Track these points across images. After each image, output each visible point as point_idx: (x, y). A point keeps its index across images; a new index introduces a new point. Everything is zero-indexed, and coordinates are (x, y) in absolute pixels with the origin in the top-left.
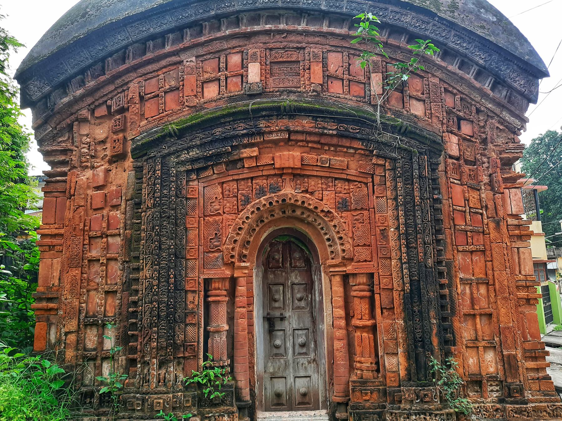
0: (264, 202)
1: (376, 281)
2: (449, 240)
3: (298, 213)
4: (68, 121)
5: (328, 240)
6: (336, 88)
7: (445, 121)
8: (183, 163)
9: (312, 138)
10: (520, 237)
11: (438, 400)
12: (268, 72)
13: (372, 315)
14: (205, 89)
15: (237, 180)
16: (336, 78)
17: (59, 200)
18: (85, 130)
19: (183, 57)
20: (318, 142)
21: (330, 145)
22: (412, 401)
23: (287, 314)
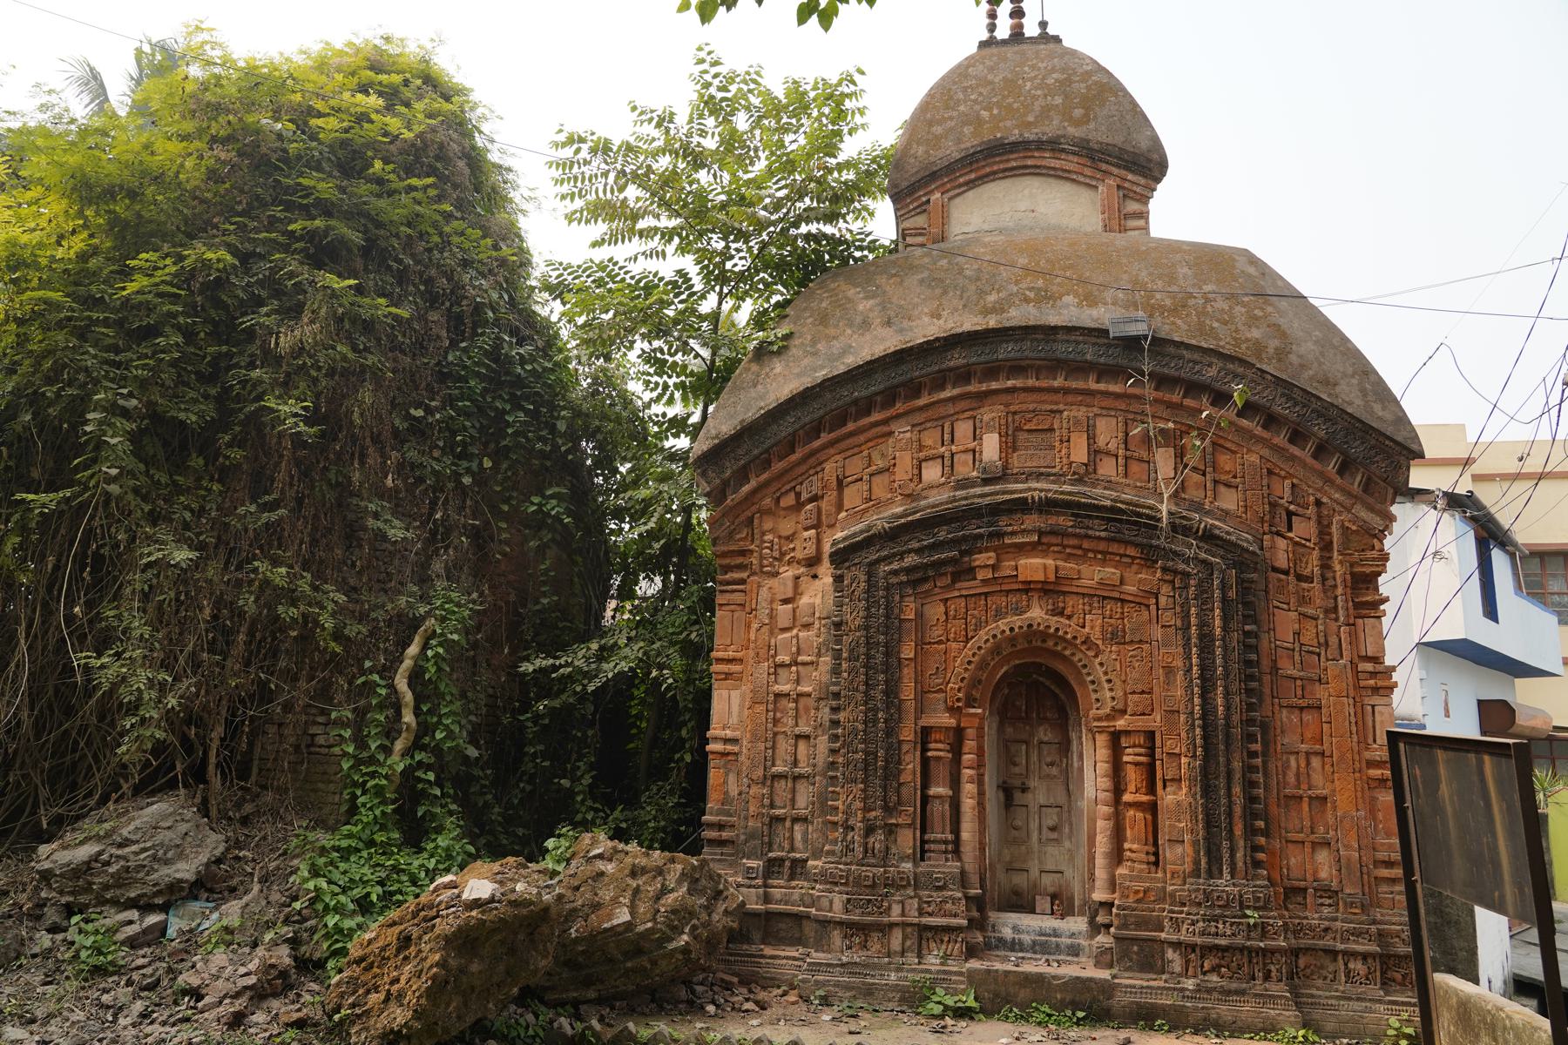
1: (1158, 743)
2: (1267, 691)
3: (1050, 643)
5: (1093, 682)
6: (1107, 468)
7: (1267, 518)
8: (895, 573)
10: (1376, 690)
11: (1236, 904)
13: (1151, 789)
14: (924, 471)
16: (1108, 453)
17: (736, 615)
19: (893, 427)
20: (1080, 547)
22: (1199, 904)
23: (1033, 783)
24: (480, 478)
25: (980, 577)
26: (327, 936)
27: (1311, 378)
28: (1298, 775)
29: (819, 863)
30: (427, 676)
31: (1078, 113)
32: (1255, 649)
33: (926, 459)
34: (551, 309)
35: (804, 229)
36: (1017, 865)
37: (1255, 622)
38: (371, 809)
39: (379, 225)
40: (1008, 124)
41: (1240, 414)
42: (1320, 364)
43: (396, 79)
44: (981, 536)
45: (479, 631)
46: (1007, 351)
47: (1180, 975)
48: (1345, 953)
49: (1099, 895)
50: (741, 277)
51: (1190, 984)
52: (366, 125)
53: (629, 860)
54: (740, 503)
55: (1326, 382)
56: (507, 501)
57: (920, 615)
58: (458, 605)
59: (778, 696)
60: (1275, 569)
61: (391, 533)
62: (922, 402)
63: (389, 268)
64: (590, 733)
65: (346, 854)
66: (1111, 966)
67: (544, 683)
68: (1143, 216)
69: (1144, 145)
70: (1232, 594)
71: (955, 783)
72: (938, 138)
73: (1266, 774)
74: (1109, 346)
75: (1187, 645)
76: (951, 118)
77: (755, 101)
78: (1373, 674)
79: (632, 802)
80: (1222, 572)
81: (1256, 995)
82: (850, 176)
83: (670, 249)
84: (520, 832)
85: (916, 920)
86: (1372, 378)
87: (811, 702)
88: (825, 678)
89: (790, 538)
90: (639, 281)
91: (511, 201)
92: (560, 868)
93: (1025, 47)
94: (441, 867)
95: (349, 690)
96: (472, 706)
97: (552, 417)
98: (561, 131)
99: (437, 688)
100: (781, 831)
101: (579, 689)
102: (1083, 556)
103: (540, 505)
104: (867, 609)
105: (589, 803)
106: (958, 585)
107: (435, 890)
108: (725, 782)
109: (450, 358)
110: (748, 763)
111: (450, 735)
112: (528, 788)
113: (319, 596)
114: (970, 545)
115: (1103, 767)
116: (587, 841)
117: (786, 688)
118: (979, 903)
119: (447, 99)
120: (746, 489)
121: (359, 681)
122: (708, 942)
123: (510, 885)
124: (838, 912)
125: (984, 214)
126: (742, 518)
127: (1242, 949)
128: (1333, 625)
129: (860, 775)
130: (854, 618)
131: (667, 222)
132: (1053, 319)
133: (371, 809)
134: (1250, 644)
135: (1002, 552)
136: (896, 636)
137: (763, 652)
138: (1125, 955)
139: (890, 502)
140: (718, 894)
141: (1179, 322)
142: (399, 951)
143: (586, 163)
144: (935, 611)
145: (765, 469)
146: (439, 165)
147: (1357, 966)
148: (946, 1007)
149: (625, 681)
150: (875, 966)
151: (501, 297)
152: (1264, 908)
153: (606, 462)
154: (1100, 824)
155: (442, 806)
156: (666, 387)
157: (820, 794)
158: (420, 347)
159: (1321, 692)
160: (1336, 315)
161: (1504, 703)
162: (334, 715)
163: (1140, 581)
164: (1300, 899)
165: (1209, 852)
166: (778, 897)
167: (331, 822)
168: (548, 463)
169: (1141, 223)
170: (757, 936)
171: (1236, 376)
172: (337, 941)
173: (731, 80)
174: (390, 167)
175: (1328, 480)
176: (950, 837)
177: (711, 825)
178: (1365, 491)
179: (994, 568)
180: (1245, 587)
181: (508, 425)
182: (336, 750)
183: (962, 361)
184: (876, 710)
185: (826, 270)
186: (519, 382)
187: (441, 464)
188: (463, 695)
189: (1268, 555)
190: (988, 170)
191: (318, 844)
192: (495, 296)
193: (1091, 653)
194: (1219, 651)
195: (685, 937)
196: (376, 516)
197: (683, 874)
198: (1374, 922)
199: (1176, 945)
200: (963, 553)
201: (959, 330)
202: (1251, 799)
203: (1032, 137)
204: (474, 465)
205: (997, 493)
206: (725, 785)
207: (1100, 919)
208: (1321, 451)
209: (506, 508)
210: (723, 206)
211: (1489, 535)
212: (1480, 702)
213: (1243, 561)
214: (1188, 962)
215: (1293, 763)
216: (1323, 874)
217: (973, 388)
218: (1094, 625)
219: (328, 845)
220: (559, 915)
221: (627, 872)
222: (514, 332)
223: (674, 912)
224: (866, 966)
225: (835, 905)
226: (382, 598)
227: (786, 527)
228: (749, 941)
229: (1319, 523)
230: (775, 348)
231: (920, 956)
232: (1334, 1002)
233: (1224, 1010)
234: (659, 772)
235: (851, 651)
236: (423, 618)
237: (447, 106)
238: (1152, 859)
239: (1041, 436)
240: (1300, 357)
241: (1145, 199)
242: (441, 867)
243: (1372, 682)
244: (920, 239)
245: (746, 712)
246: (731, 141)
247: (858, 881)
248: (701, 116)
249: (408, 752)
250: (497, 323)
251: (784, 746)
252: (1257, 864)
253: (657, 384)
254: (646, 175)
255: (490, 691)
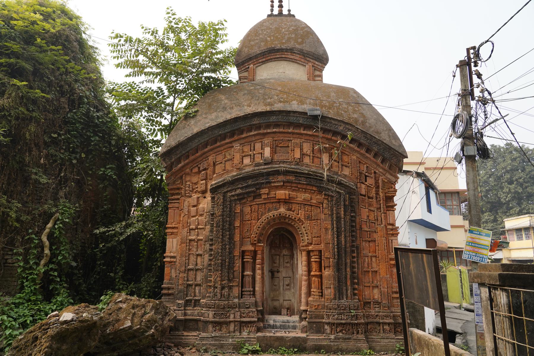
0: (271, 215)
1: (323, 254)
2: (358, 236)
3: (287, 220)
4: (181, 174)
6: (307, 160)
8: (233, 196)
9: (295, 185)
10: (393, 235)
12: (274, 152)
13: (320, 270)
15: (258, 204)
16: (307, 155)
17: (176, 211)
18: (188, 179)
19: (234, 144)
20: (297, 187)
21: (302, 189)
22: (336, 309)
24: (81, 161)
25: (263, 197)
26: (6, 338)
27: (373, 131)
28: (368, 264)
29: (204, 301)
30: (55, 235)
31: (300, 40)
32: (354, 221)
33: (245, 156)
34: (109, 100)
35: (206, 74)
36: (275, 298)
37: (354, 213)
38: (30, 287)
39: (41, 64)
40: (276, 42)
41: (350, 143)
42: (376, 126)
43: (49, 10)
44: (263, 183)
45: (79, 218)
46: (273, 119)
47: (329, 334)
48: (383, 323)
49: (303, 308)
50: (182, 91)
51: (332, 337)
52: (36, 26)
53: (132, 302)
54: (178, 171)
55: (377, 132)
56: (91, 170)
57: (242, 211)
58: (69, 208)
59: (190, 240)
60: (361, 195)
61: (42, 180)
62: (243, 136)
63: (44, 80)
64: (122, 256)
65: (17, 305)
66: (306, 332)
67: (103, 237)
68: (321, 76)
69: (321, 52)
70: (347, 203)
71: (254, 270)
72: (252, 46)
73: (358, 264)
74: (308, 118)
75: (332, 221)
76: (257, 39)
77: (188, 29)
78: (392, 229)
79: (138, 281)
80: (344, 195)
81: (354, 339)
82: (220, 56)
83: (156, 80)
84: (94, 293)
85: (239, 320)
86: (392, 131)
87: (202, 242)
88: (208, 234)
89: (196, 184)
90: (144, 91)
91: (97, 60)
92: (105, 307)
93: (283, 17)
94: (58, 308)
95: (22, 241)
96: (74, 246)
97: (110, 139)
98: (113, 33)
99: (59, 240)
100: (191, 290)
101: (117, 239)
102: (298, 190)
103: (104, 171)
104: (223, 209)
105: (121, 282)
106: (255, 200)
107: (49, 318)
108: (171, 272)
109: (69, 115)
110: (179, 265)
111: (65, 258)
112: (98, 277)
113: (10, 205)
114: (260, 186)
115: (304, 263)
116: (117, 296)
117: (193, 238)
118: (262, 312)
119: (71, 20)
120: (180, 165)
121: (26, 238)
122: (162, 331)
123: (81, 314)
124: (211, 318)
125: (267, 72)
126: (179, 176)
127: (350, 324)
128: (379, 214)
129: (220, 268)
130: (218, 212)
131: (155, 70)
132: (289, 109)
133: (30, 287)
134: (353, 220)
135: (271, 188)
136: (233, 218)
137: (185, 225)
138: (311, 328)
139: (232, 171)
140: (166, 314)
141: (331, 111)
142: (33, 343)
143: (123, 45)
144: (247, 209)
145: (187, 159)
146: (66, 43)
147: (386, 327)
148: (249, 350)
149: (138, 236)
150: (224, 337)
151: (90, 94)
152: (357, 309)
153: (131, 156)
154: (303, 283)
155: (60, 285)
156: (154, 130)
157: (205, 276)
158: (56, 111)
159: (375, 236)
160: (380, 111)
161: (433, 239)
162: (15, 251)
163: (317, 199)
164: (369, 306)
165: (339, 291)
166: (189, 313)
167: (13, 293)
168: (108, 156)
169: (320, 78)
170: (181, 328)
171: (349, 130)
172: (10, 340)
173: (180, 21)
174: (44, 41)
175: (378, 165)
176: (251, 289)
177: (165, 288)
178: (389, 169)
179: (268, 194)
180: (351, 201)
181: (92, 141)
182: (16, 265)
183: (258, 122)
184: (225, 245)
185: (212, 89)
186: (97, 126)
187: (63, 155)
188: (71, 242)
189: (359, 190)
190: (269, 58)
191: (5, 302)
192: (88, 93)
193: (300, 224)
194: (343, 222)
195: (153, 330)
196: (36, 174)
197: (152, 307)
198: (392, 312)
199: (328, 324)
200: (257, 189)
201: (257, 111)
202: (353, 273)
203: (284, 47)
204: (78, 156)
205: (269, 168)
206: (170, 273)
207: (303, 316)
208: (376, 155)
209: (90, 172)
210: (175, 65)
211: (429, 186)
212: (426, 239)
213: (351, 192)
214: (332, 329)
215: (367, 260)
216: (376, 297)
217: (261, 131)
218: (302, 214)
219: (10, 302)
220: (101, 325)
221: (131, 307)
222: (96, 107)
223: (149, 321)
224: (220, 337)
225: (210, 315)
226: (38, 206)
227: (195, 179)
228: (178, 330)
229: (375, 179)
230: (192, 115)
231: (240, 332)
232: (379, 340)
233: (344, 345)
234: (149, 270)
235: (217, 224)
236: (54, 213)
237: (72, 22)
238: (320, 294)
239: (285, 149)
240: (369, 124)
241: (321, 71)
242: (58, 308)
243: (391, 232)
244: (245, 80)
245: (179, 247)
246: (179, 42)
247: (218, 307)
248: (168, 33)
249: (45, 265)
250: (88, 103)
251: (192, 258)
252: (355, 294)
253: (151, 129)
254: (146, 52)
255: (83, 241)
